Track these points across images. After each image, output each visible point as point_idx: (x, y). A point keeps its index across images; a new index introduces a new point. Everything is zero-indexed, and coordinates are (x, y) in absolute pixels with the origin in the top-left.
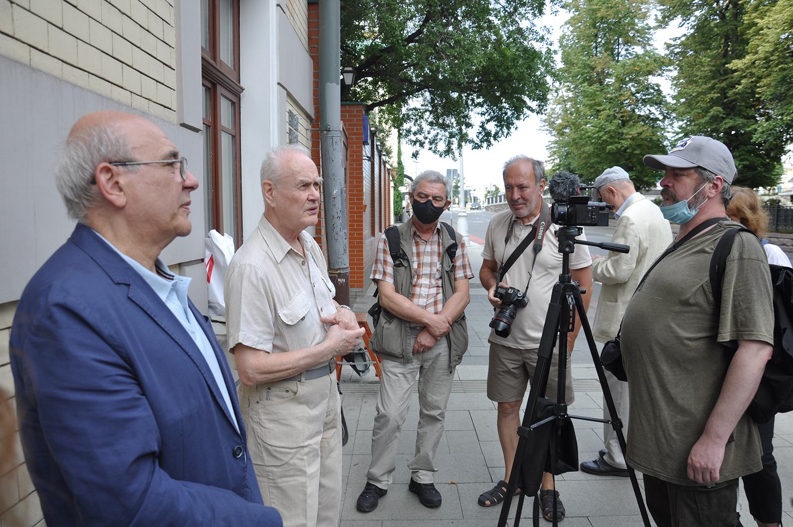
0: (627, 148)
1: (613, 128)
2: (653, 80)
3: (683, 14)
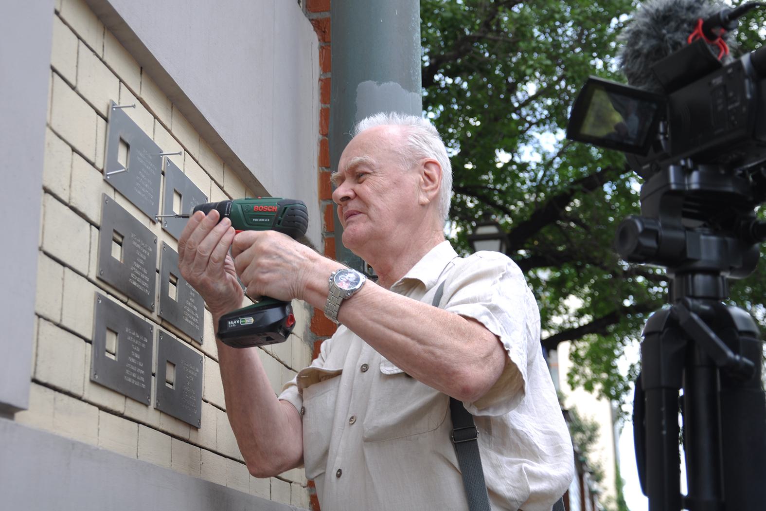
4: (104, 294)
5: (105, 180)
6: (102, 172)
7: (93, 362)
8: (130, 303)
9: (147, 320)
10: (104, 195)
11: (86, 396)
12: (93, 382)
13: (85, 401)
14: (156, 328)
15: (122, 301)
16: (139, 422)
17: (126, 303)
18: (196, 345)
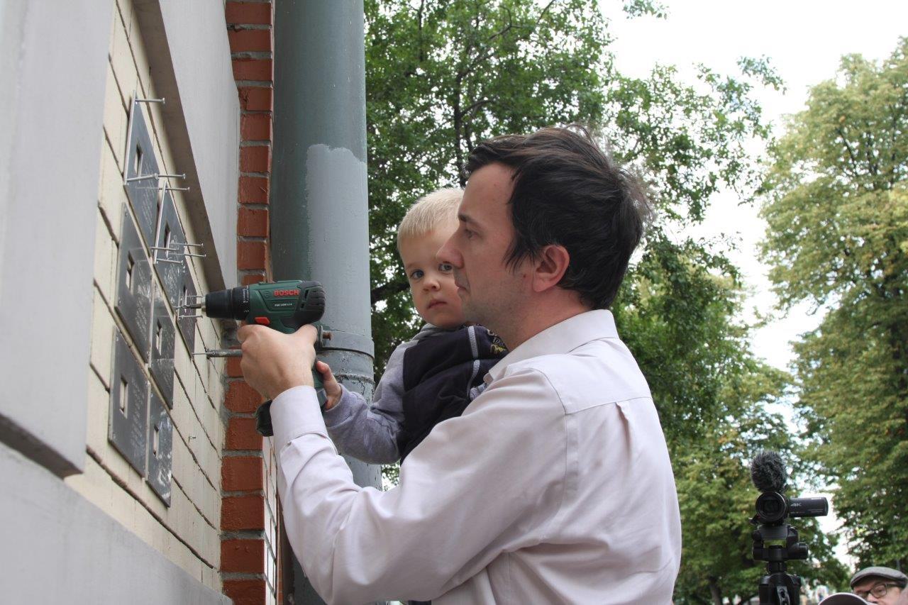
0: (740, 527)
1: (714, 492)
2: (769, 409)
3: (817, 294)
5: (124, 187)
12: (110, 443)
13: (104, 467)
14: (149, 383)
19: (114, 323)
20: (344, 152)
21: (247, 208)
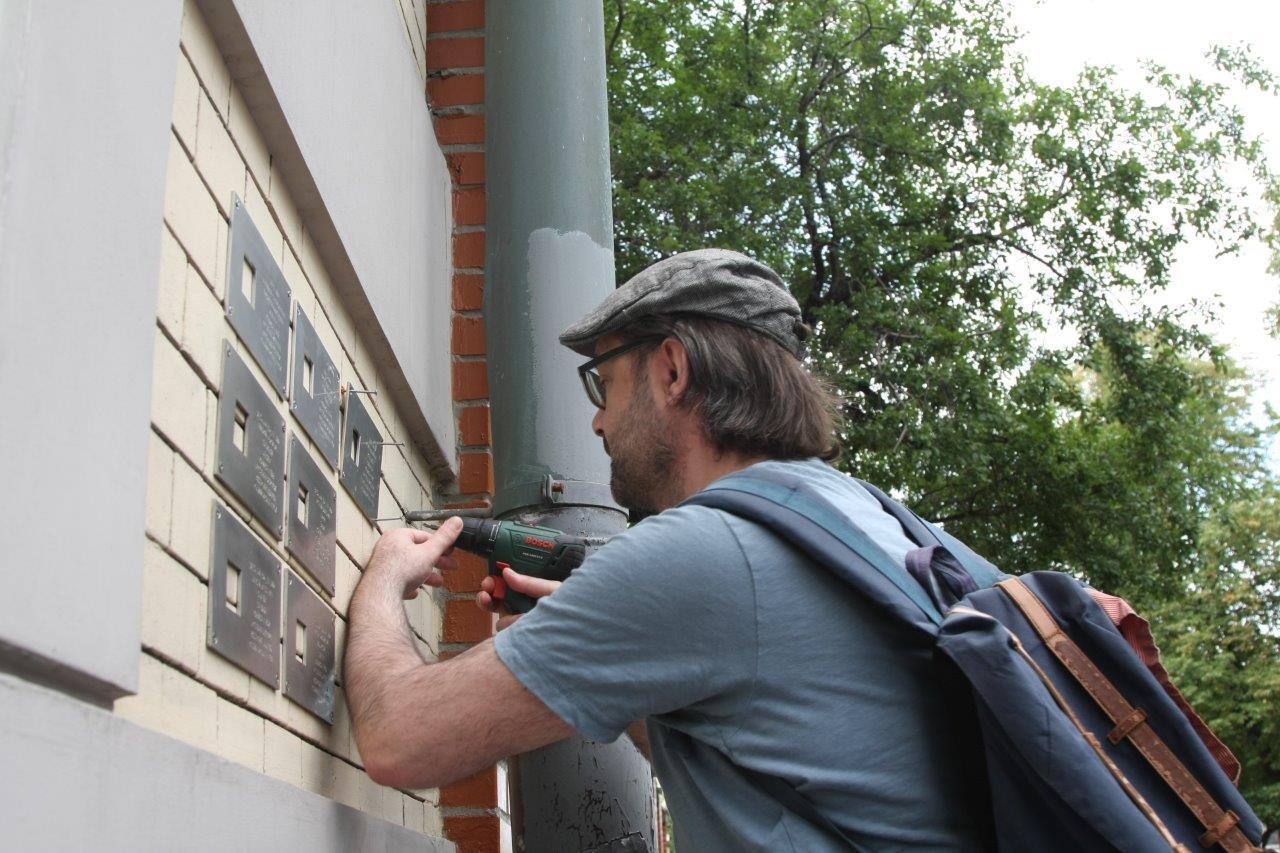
4: (223, 504)
5: (226, 318)
6: (222, 304)
7: (211, 616)
8: (254, 523)
9: (274, 553)
10: (226, 342)
11: (201, 674)
12: (211, 650)
13: (201, 681)
14: (285, 566)
15: (243, 519)
16: (264, 716)
17: (248, 523)
18: (326, 597)
19: (215, 496)
20: (578, 236)
21: (465, 317)
